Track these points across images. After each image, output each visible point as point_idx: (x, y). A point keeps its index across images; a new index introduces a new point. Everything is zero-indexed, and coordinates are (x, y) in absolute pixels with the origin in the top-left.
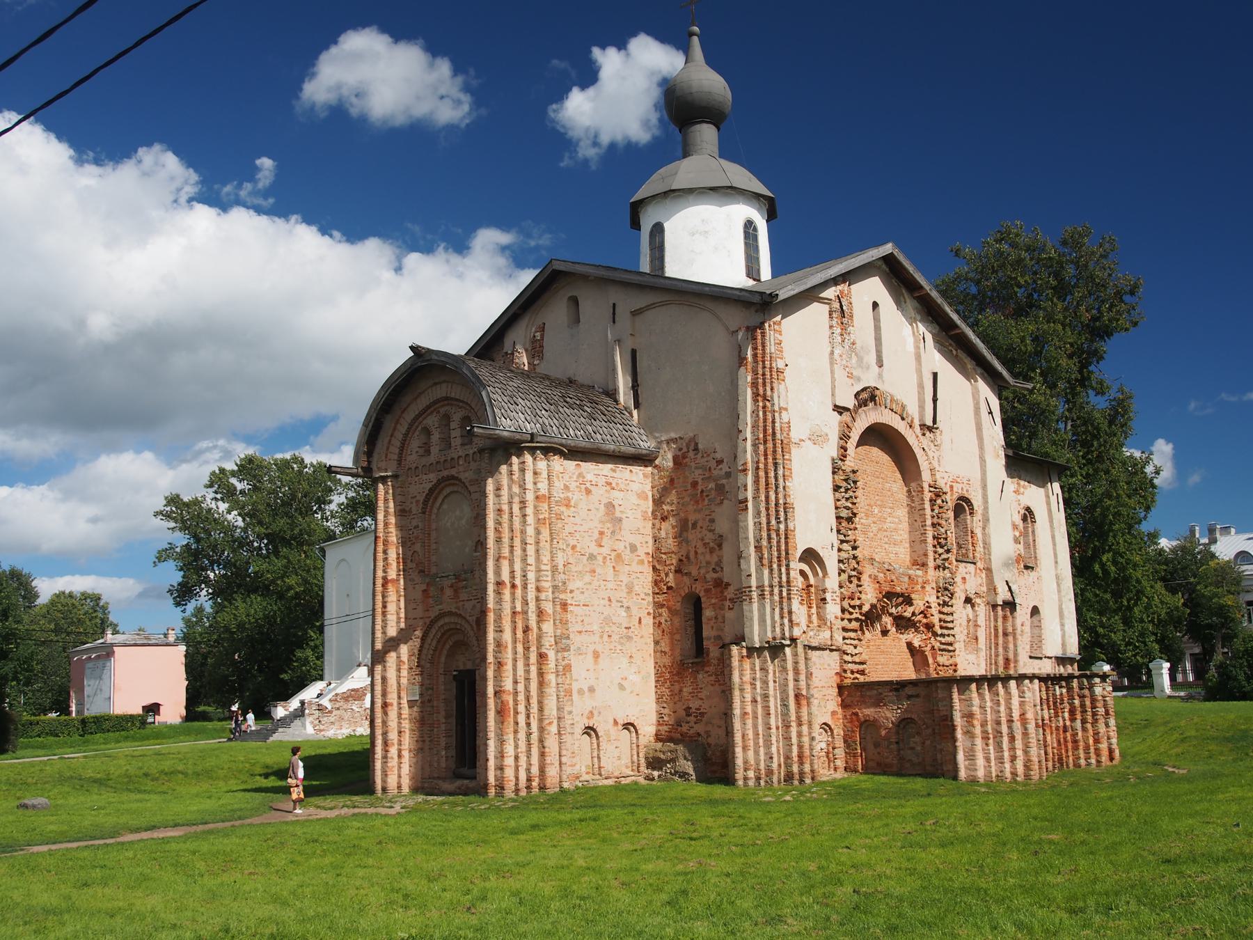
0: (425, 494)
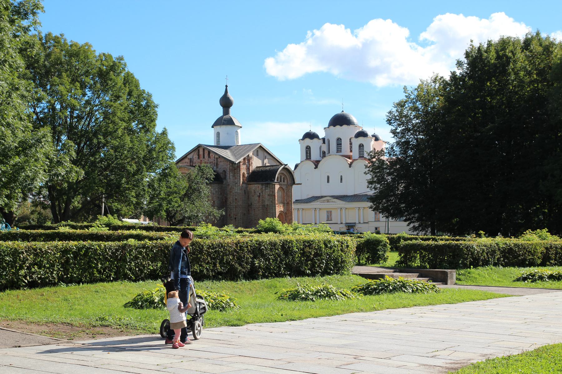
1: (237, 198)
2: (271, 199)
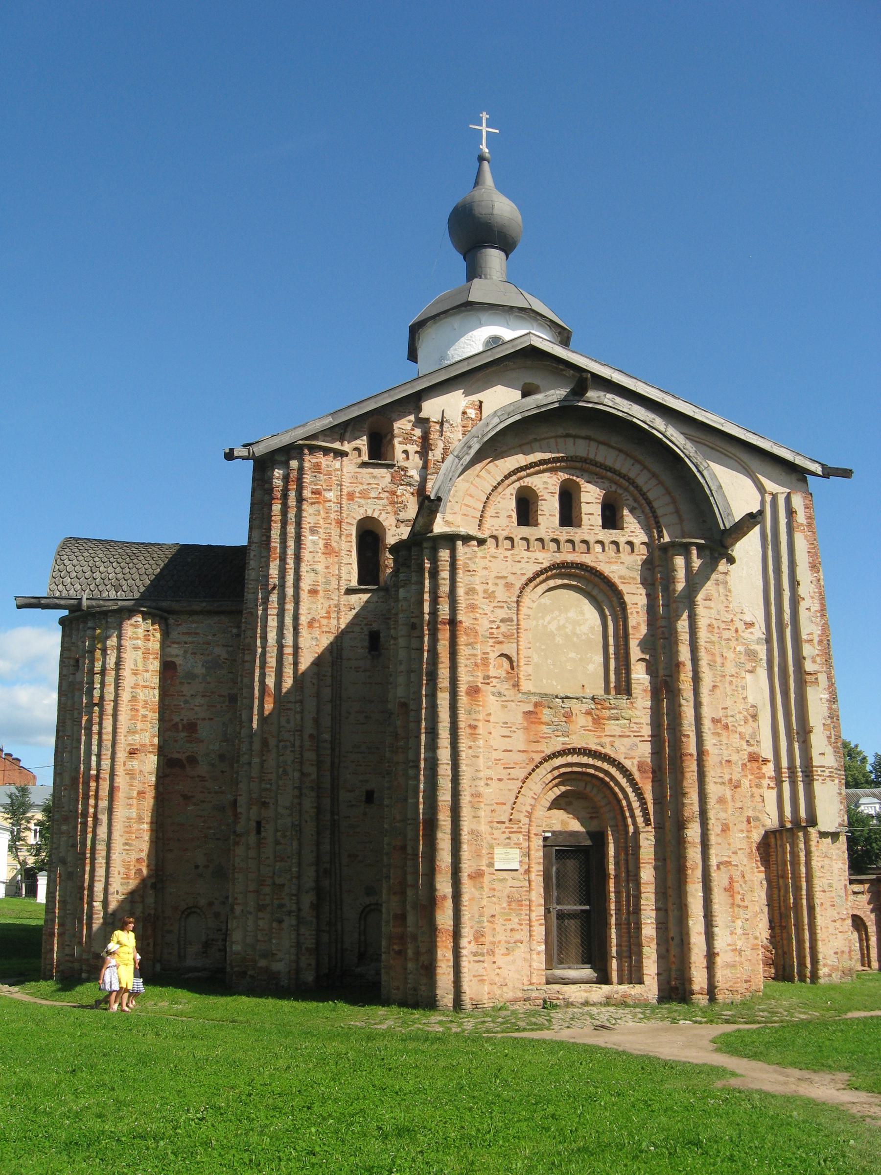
0: (524, 579)
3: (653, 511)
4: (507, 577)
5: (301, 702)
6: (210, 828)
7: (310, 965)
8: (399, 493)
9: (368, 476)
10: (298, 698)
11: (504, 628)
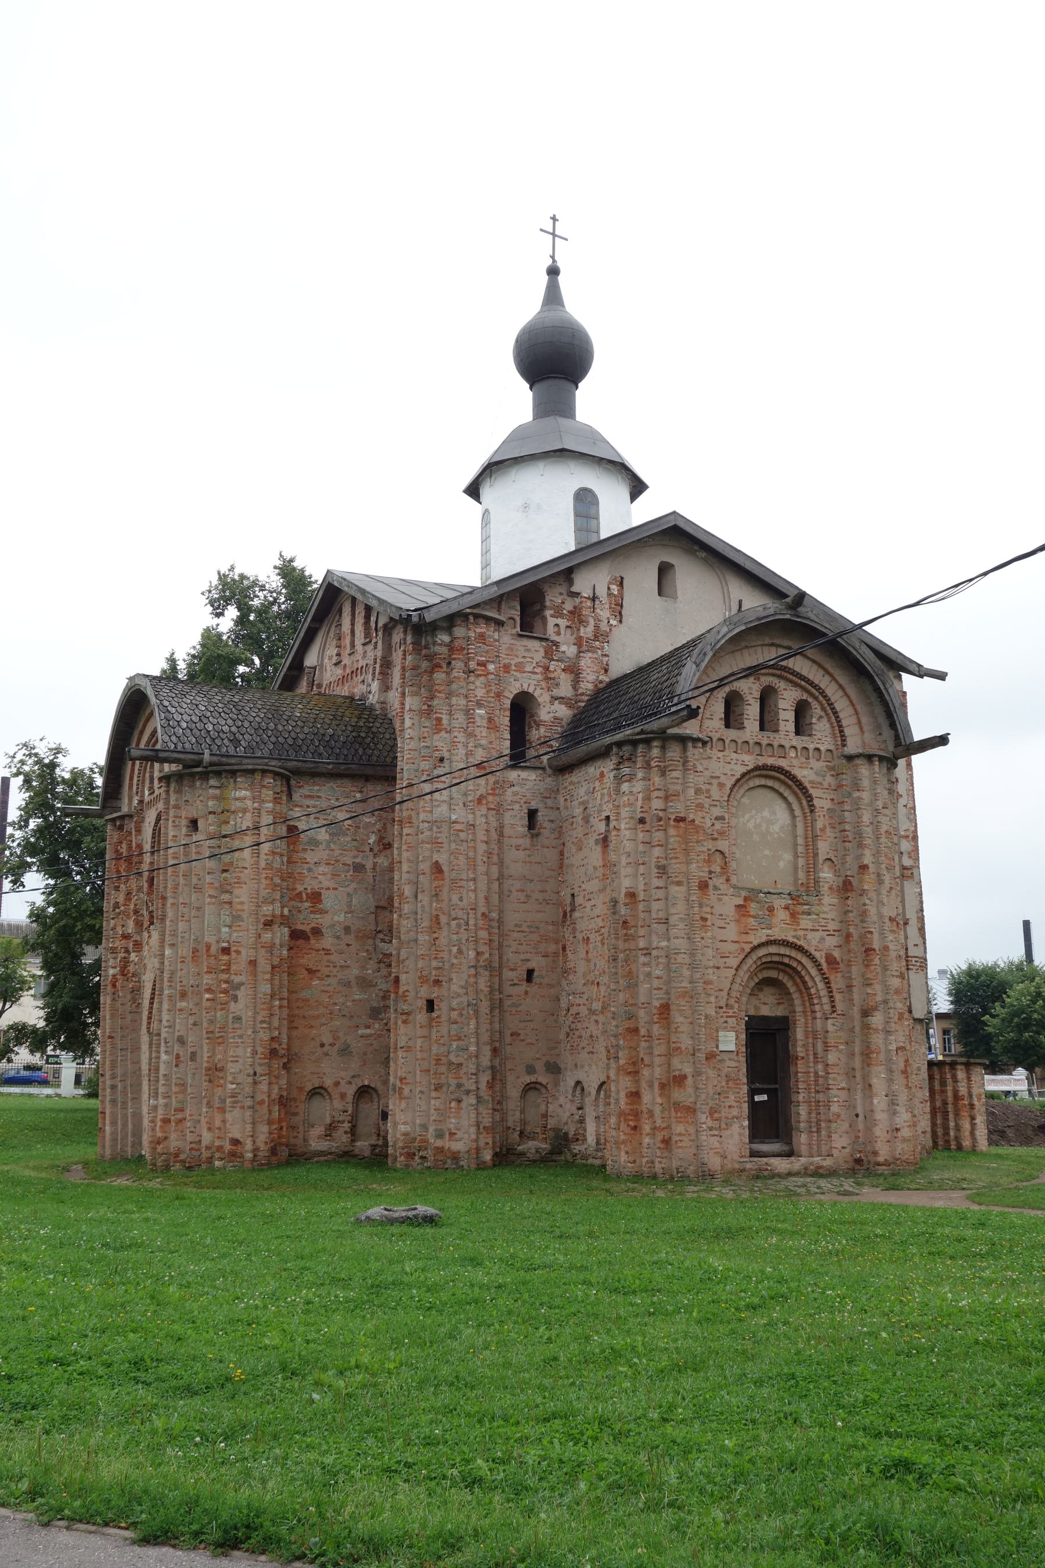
0: (734, 779)
1: (442, 858)
2: (657, 852)
3: (839, 721)
4: (719, 777)
5: (474, 879)
6: (335, 1004)
7: (488, 1143)
8: (552, 668)
9: (522, 649)
10: (472, 876)
11: (718, 826)
